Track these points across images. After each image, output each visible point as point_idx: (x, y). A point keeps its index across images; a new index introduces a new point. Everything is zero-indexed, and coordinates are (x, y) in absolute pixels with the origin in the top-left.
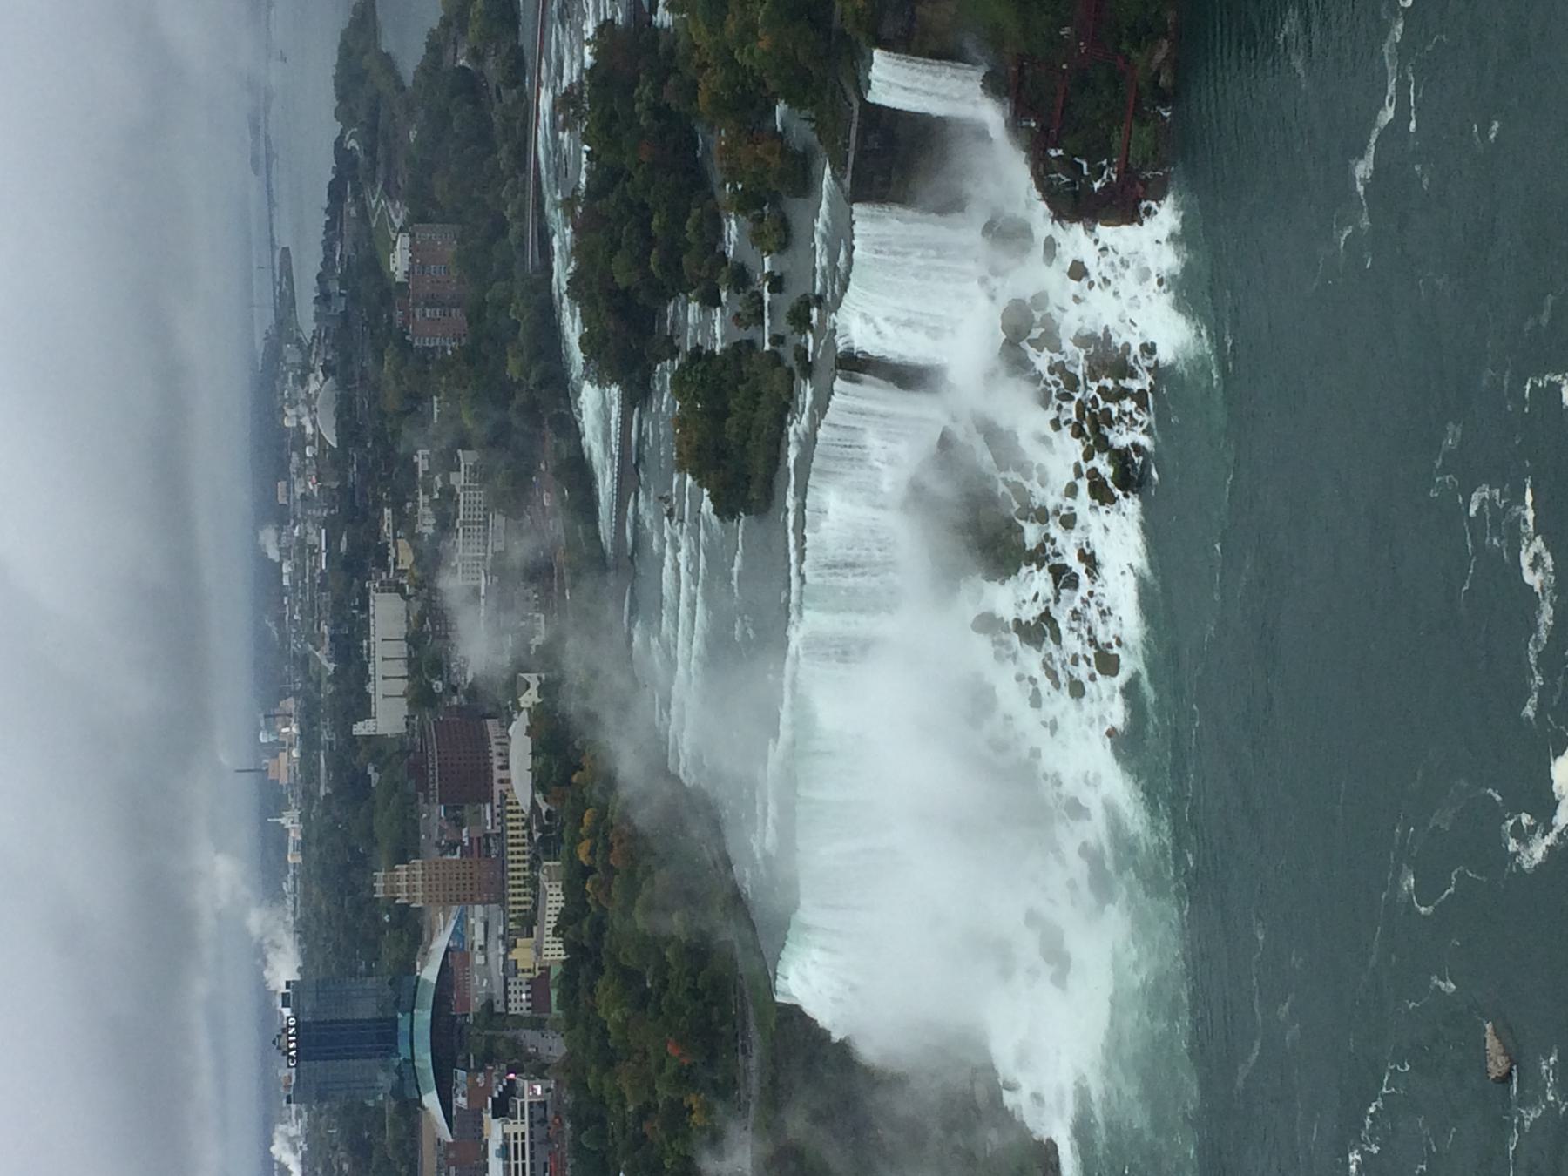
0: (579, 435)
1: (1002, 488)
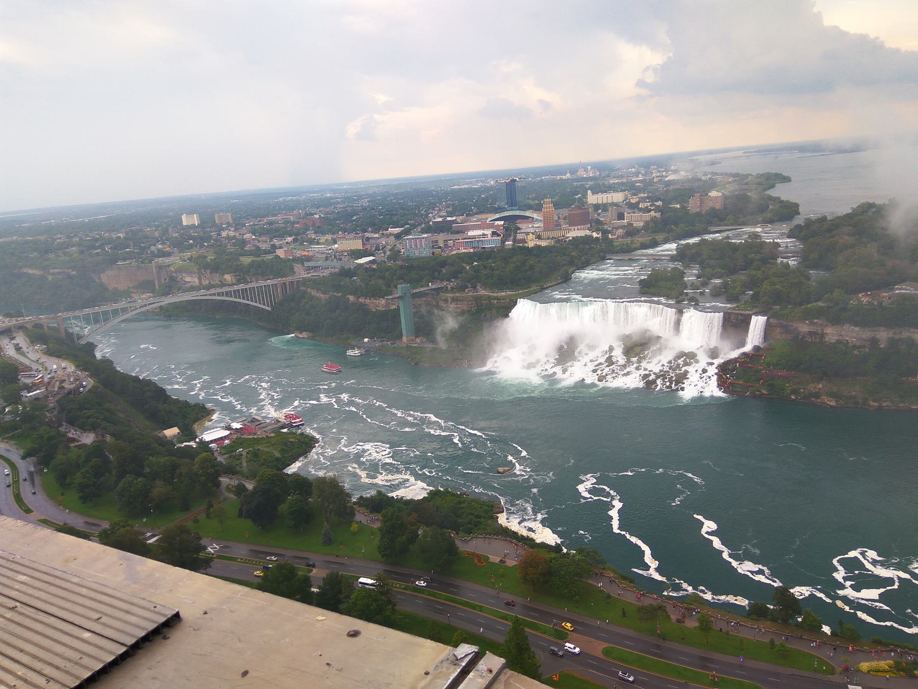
0: (664, 244)
1: (646, 352)
